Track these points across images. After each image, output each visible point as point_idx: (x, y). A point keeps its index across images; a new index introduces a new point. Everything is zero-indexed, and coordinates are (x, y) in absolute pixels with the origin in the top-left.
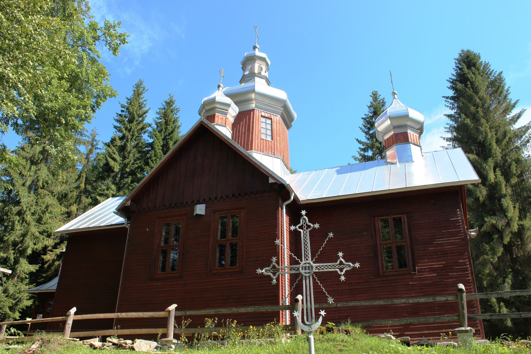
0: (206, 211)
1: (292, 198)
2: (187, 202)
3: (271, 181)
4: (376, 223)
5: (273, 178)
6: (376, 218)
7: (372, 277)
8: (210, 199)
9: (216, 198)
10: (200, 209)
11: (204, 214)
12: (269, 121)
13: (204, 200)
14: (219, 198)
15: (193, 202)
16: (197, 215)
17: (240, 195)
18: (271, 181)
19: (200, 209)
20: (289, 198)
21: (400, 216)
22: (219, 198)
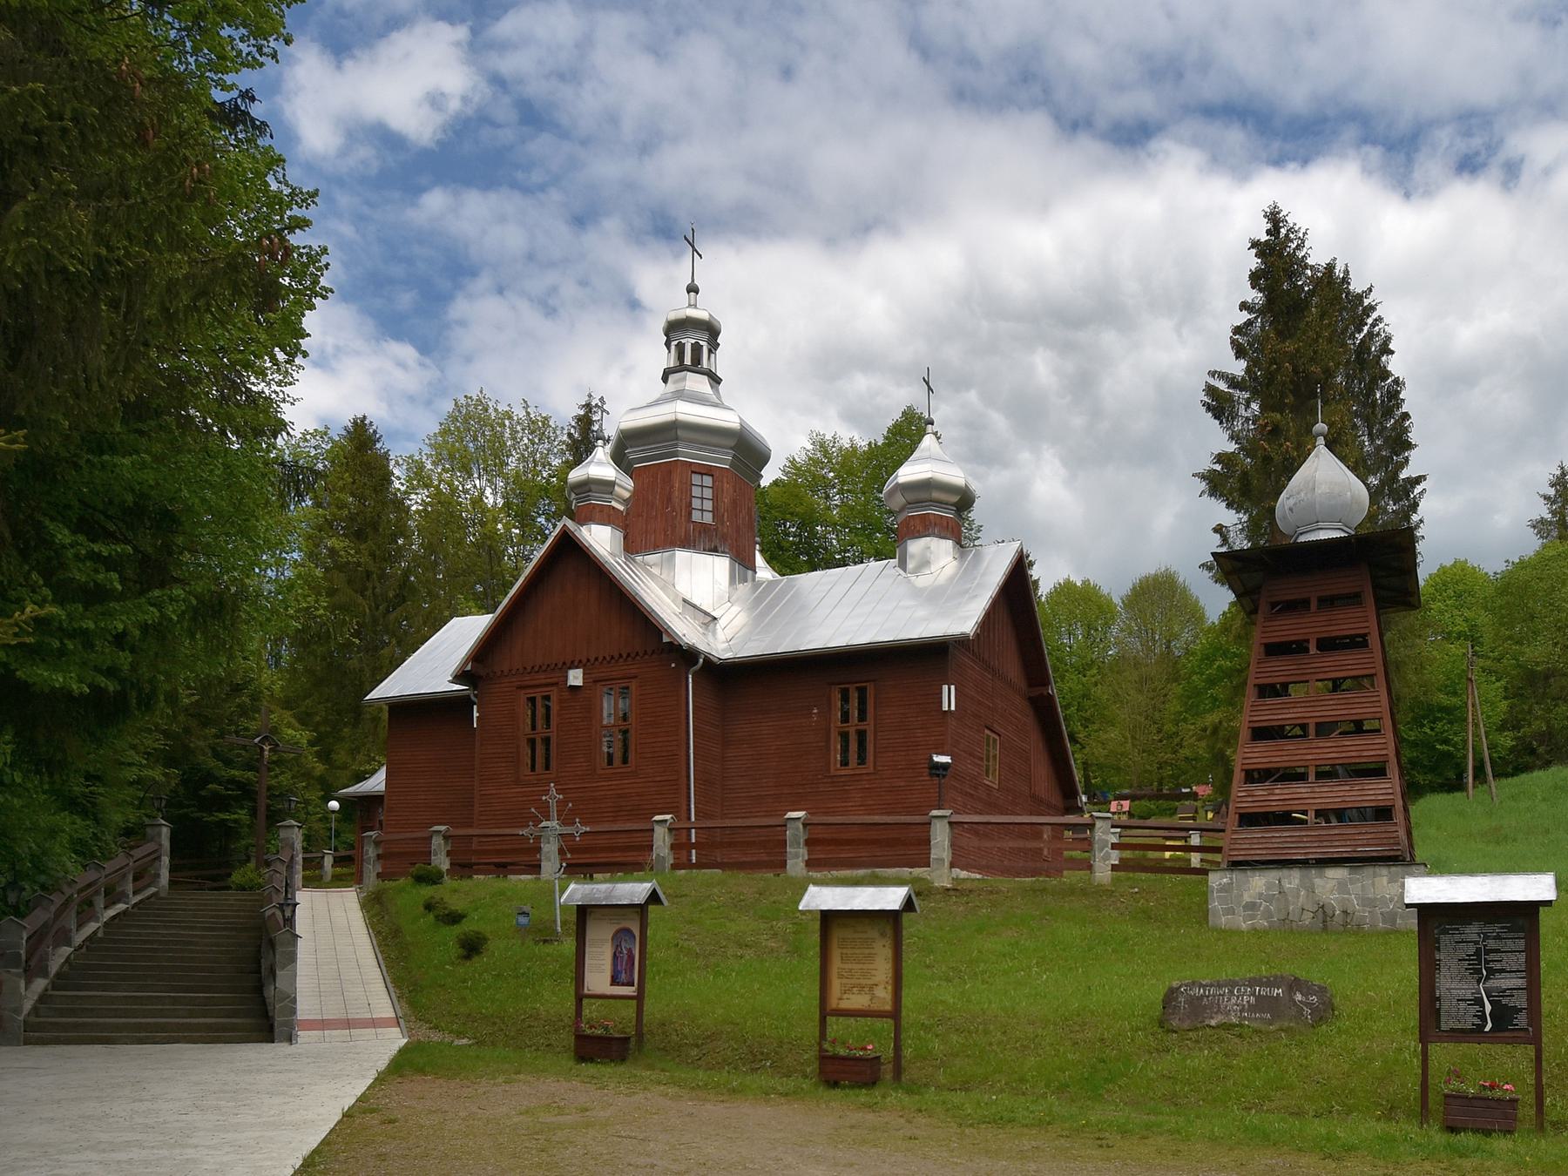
0: (584, 679)
1: (701, 660)
2: (556, 665)
3: (666, 639)
4: (832, 695)
5: (669, 635)
6: (833, 686)
7: (820, 777)
8: (588, 660)
9: (596, 659)
10: (576, 677)
11: (581, 684)
12: (708, 481)
13: (580, 661)
14: (600, 659)
15: (564, 663)
16: (570, 686)
17: (629, 655)
18: (666, 639)
19: (576, 678)
20: (697, 662)
21: (864, 684)
22: (600, 659)
